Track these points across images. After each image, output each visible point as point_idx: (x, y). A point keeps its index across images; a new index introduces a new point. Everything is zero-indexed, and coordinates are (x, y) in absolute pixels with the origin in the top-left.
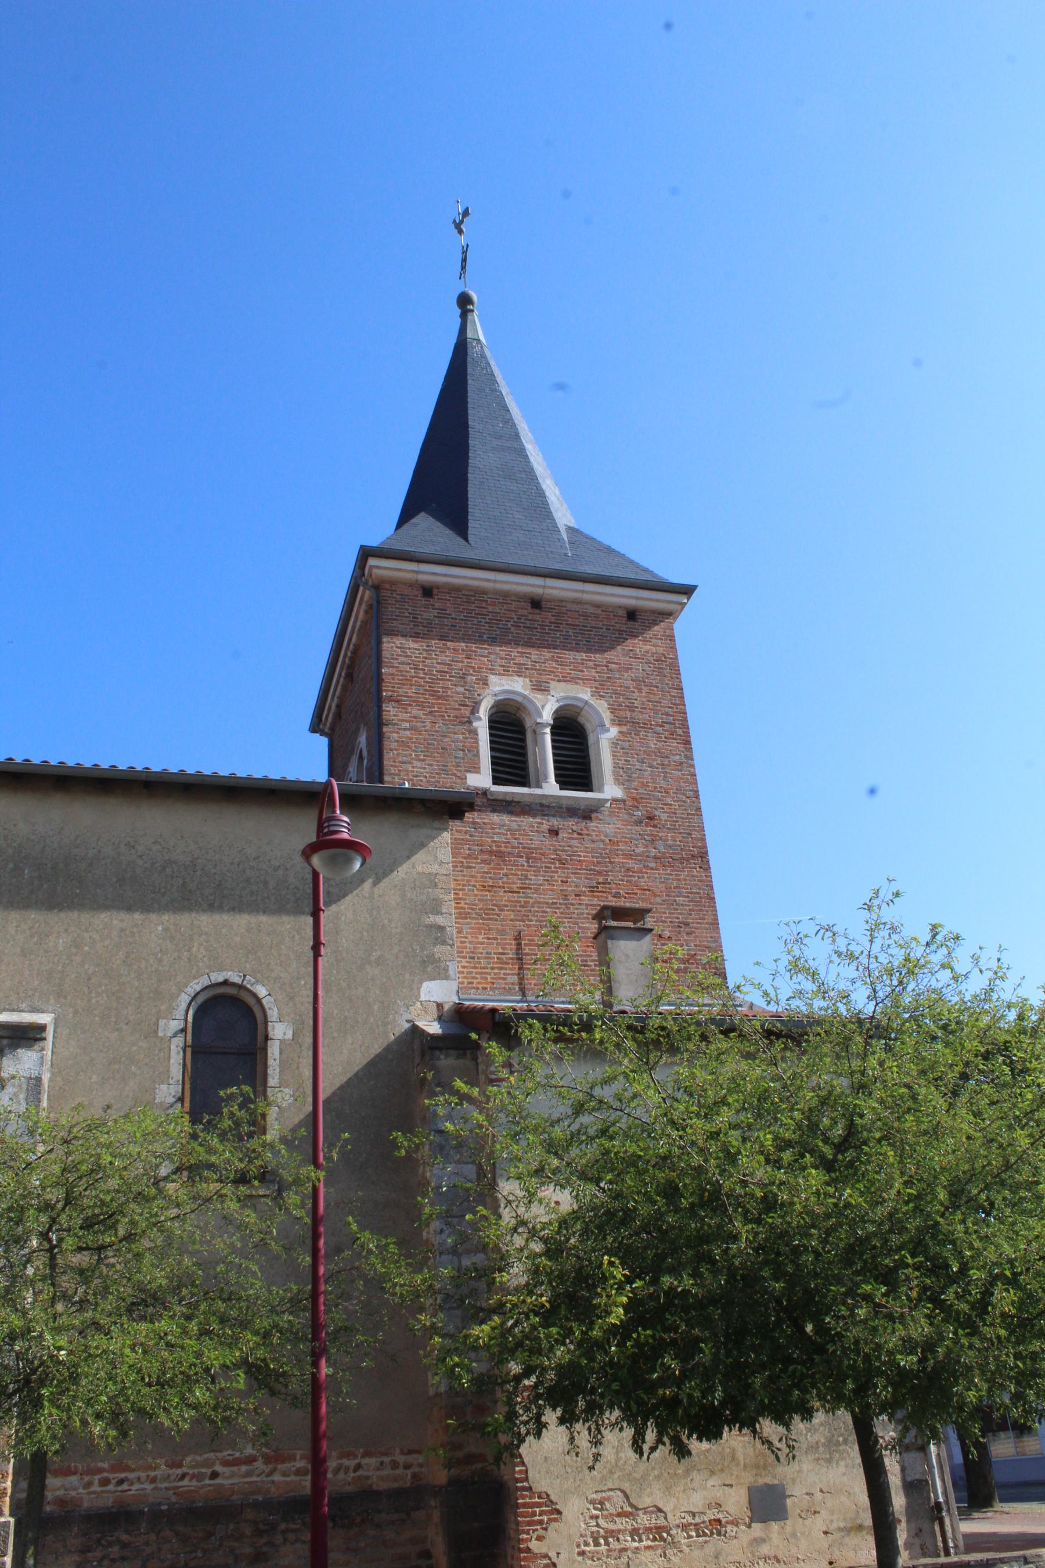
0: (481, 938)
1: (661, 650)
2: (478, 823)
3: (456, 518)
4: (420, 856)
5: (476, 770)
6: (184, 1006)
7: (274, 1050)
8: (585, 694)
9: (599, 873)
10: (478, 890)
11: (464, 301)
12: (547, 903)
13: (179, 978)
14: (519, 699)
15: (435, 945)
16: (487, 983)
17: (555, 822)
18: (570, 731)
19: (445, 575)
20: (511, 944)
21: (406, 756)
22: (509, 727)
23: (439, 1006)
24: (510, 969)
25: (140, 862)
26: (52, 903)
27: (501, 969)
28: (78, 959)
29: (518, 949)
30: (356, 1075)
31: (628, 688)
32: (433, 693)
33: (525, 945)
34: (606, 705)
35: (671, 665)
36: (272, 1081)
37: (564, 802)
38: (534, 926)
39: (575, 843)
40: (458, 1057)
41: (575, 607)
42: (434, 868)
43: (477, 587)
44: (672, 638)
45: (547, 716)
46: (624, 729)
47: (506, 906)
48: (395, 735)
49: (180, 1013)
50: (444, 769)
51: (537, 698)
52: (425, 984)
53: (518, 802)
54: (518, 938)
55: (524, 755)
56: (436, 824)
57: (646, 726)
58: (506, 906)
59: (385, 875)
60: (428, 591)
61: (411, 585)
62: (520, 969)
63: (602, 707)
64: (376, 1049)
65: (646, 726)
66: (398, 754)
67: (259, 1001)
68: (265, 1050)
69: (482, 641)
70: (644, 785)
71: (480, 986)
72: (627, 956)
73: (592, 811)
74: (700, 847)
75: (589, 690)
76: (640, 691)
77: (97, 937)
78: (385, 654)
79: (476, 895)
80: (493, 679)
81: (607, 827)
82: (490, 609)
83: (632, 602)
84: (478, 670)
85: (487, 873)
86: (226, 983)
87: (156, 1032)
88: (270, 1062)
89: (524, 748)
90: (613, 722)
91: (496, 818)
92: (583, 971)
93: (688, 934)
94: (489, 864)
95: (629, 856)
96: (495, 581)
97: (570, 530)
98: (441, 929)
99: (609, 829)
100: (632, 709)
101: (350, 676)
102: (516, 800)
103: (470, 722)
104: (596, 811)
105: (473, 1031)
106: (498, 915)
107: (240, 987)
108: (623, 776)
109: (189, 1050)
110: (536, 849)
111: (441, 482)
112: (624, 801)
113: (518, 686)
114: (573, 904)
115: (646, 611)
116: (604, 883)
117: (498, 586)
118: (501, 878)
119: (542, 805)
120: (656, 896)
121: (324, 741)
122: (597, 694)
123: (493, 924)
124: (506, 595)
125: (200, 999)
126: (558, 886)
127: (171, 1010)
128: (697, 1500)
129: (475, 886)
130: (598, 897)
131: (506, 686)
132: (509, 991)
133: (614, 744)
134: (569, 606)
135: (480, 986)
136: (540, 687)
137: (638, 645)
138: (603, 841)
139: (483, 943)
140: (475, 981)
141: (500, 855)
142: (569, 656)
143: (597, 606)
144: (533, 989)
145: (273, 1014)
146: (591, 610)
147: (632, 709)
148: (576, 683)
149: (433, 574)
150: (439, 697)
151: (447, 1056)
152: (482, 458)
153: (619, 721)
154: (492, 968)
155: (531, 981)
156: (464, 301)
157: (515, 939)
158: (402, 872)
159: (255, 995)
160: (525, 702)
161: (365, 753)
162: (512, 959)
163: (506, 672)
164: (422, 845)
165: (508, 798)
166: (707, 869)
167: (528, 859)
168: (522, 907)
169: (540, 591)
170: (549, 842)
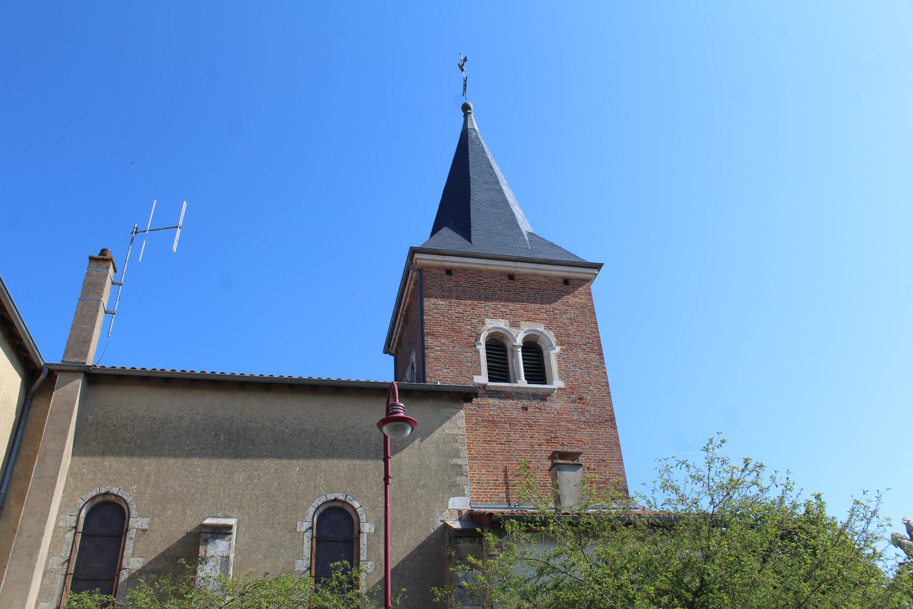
0: (483, 471)
3: (465, 231)
4: (447, 424)
5: (479, 373)
6: (311, 513)
7: (364, 539)
8: (541, 328)
9: (552, 432)
11: (466, 108)
13: (309, 497)
14: (503, 332)
15: (456, 476)
17: (525, 402)
18: (533, 349)
22: (497, 348)
23: (460, 512)
25: (287, 430)
26: (237, 455)
28: (251, 487)
30: (412, 553)
32: (453, 330)
36: (362, 558)
37: (530, 391)
39: (537, 414)
40: (471, 542)
41: (533, 278)
42: (456, 431)
44: (590, 294)
45: (519, 341)
46: (564, 347)
49: (309, 518)
51: (513, 331)
52: (451, 499)
54: (505, 471)
55: (507, 364)
56: (456, 405)
57: (577, 345)
59: (427, 436)
60: (449, 272)
61: (439, 268)
63: (551, 335)
64: (423, 537)
65: (577, 345)
67: (355, 510)
68: (358, 539)
69: (480, 299)
70: (577, 380)
72: (569, 480)
76: (573, 325)
77: (261, 474)
78: (426, 308)
80: (487, 321)
81: (556, 405)
82: (485, 280)
83: (566, 274)
84: (479, 316)
86: (335, 500)
87: (295, 529)
88: (362, 546)
89: (506, 360)
90: (557, 344)
91: (491, 401)
95: (570, 422)
97: (529, 233)
98: (460, 466)
99: (557, 406)
100: (568, 335)
101: (406, 321)
103: (475, 346)
104: (549, 395)
105: (479, 525)
107: (344, 502)
108: (564, 374)
109: (314, 540)
111: (455, 209)
113: (502, 324)
117: (490, 268)
119: (518, 393)
121: (392, 358)
122: (548, 328)
123: (491, 463)
124: (493, 273)
125: (321, 510)
126: (528, 440)
127: (304, 516)
131: (493, 324)
132: (500, 502)
133: (558, 356)
136: (515, 325)
137: (570, 299)
141: (494, 422)
142: (532, 306)
145: (363, 518)
146: (543, 279)
147: (568, 335)
150: (456, 332)
151: (464, 542)
152: (478, 195)
153: (560, 343)
156: (466, 108)
158: (437, 434)
159: (353, 507)
160: (506, 334)
161: (415, 365)
163: (495, 316)
164: (449, 418)
166: (615, 428)
167: (510, 424)
169: (513, 269)
170: (522, 414)
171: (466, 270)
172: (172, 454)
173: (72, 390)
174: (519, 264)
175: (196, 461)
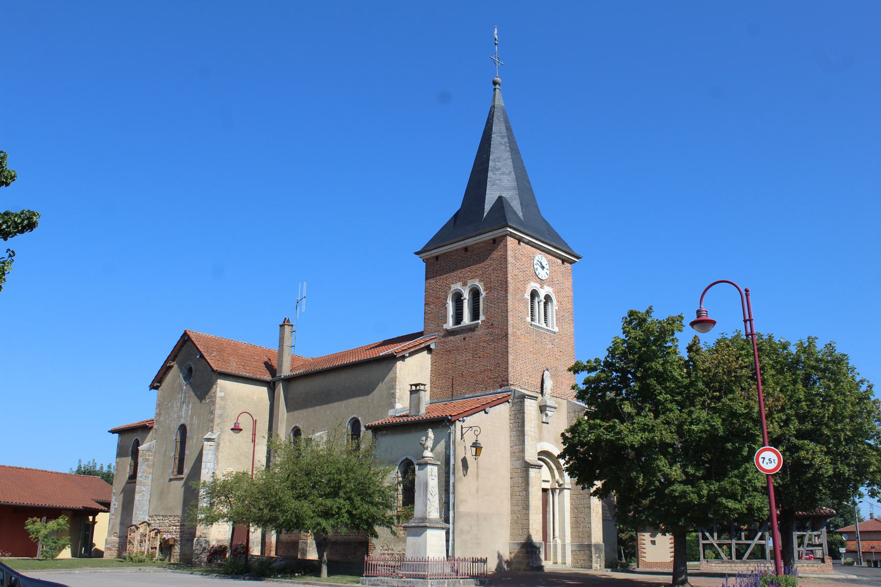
17: (465, 335)
26: (327, 402)
60: (437, 258)
61: (433, 258)
90: (485, 290)
113: (458, 286)
124: (457, 250)
128: (400, 548)
136: (465, 284)
137: (496, 254)
141: (450, 351)
142: (474, 267)
143: (484, 242)
171: (445, 254)
172: (311, 407)
173: (280, 388)
175: (317, 408)
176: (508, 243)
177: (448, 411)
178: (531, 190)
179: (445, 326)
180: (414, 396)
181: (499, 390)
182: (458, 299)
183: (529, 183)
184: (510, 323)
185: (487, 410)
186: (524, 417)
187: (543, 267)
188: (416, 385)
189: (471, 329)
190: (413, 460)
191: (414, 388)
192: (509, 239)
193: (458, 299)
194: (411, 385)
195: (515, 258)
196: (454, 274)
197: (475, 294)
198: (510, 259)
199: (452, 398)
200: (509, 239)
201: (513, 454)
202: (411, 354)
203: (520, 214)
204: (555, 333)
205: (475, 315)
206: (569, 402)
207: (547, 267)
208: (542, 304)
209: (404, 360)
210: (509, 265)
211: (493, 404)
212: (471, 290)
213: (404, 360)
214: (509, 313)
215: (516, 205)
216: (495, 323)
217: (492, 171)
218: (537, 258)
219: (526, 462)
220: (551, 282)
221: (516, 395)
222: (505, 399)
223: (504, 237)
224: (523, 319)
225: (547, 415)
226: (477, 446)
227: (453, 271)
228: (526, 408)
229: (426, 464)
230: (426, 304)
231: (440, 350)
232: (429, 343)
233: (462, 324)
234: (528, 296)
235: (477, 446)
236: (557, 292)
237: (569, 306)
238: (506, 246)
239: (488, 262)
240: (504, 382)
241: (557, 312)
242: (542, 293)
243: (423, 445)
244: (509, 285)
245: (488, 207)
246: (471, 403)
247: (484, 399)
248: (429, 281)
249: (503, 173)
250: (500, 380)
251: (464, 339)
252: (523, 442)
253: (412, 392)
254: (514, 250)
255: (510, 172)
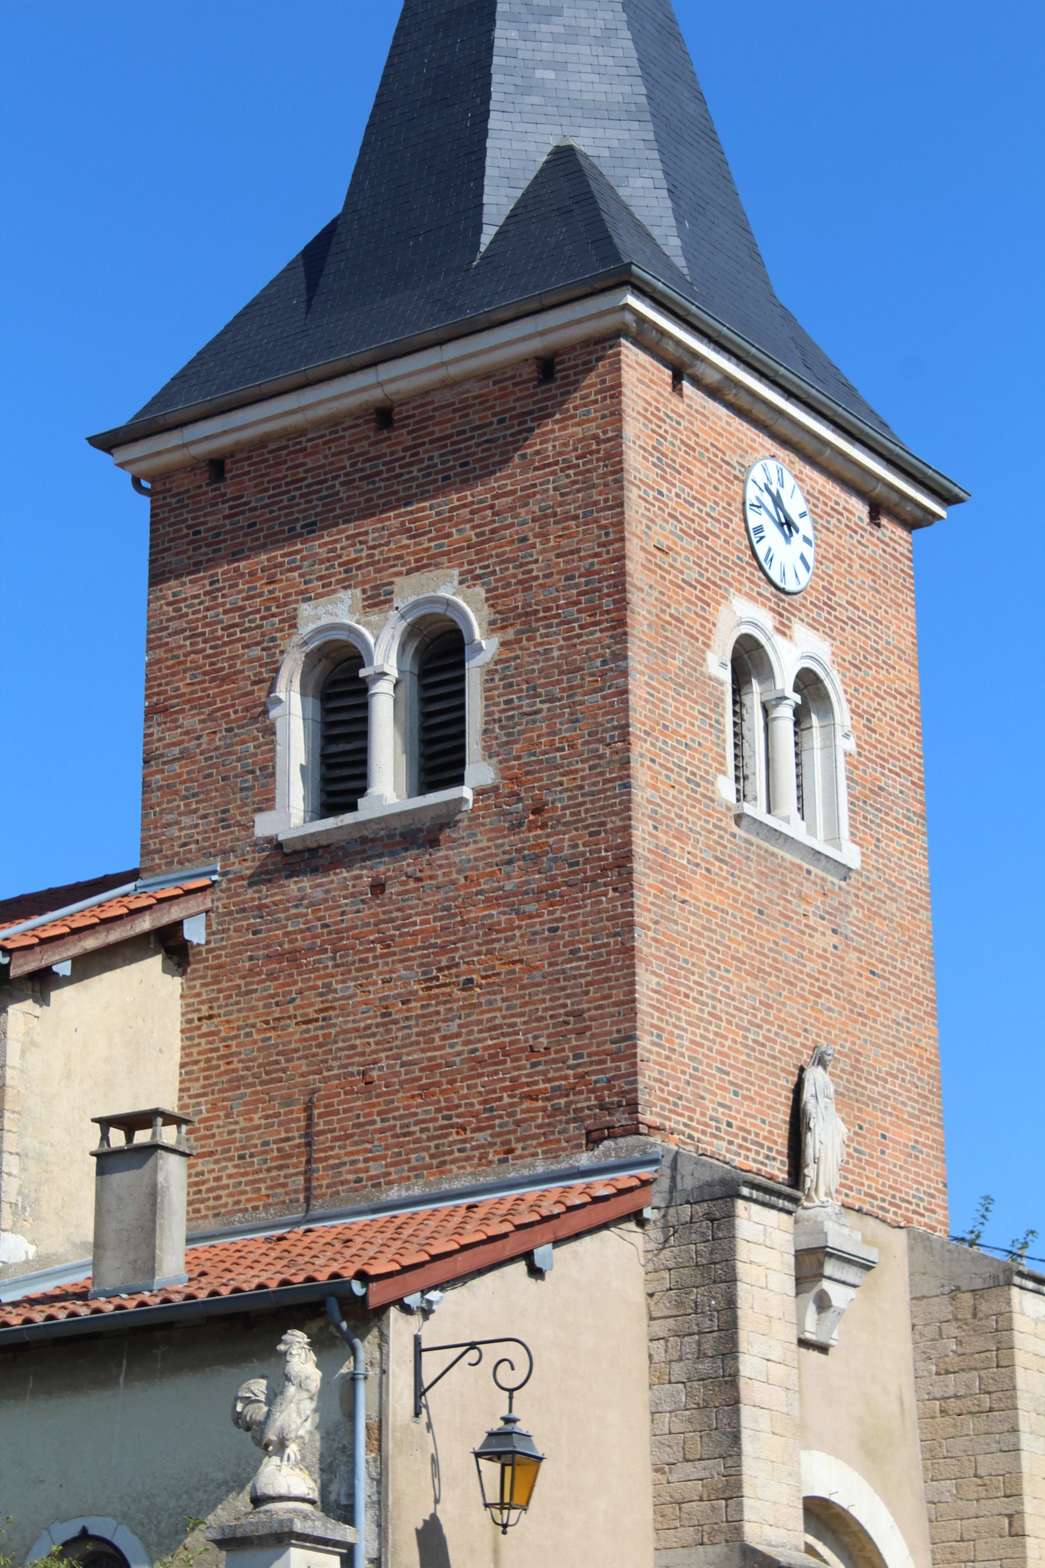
1: (592, 428)
2: (266, 906)
9: (443, 949)
10: (259, 1031)
12: (357, 1030)
16: (259, 1199)
17: (383, 868)
19: (225, 433)
20: (298, 1120)
21: (171, 811)
24: (295, 1166)
27: (280, 1168)
29: (308, 1126)
31: (525, 539)
33: (320, 1116)
34: (483, 595)
35: (608, 456)
37: (395, 824)
38: (337, 1077)
41: (449, 396)
43: (285, 429)
46: (510, 634)
47: (296, 1050)
48: (158, 777)
50: (225, 822)
53: (329, 846)
54: (308, 1108)
58: (296, 1050)
60: (216, 467)
61: (192, 467)
62: (308, 1162)
66: (162, 811)
69: (291, 539)
71: (249, 1206)
72: (120, 1198)
73: (441, 828)
74: (618, 847)
75: (456, 572)
76: (544, 536)
79: (255, 1042)
80: (306, 610)
83: (536, 345)
85: (272, 996)
90: (493, 627)
92: (400, 1145)
93: (580, 1033)
94: (277, 979)
95: (491, 902)
96: (302, 409)
102: (324, 843)
103: (265, 712)
104: (448, 825)
106: (284, 1070)
110: (348, 929)
112: (495, 789)
113: (339, 611)
114: (395, 1022)
115: (573, 348)
116: (448, 968)
117: (312, 414)
118: (293, 1000)
119: (364, 840)
120: (531, 969)
123: (279, 1091)
124: (334, 422)
129: (253, 1026)
130: (437, 996)
133: (490, 674)
134: (439, 399)
135: (249, 1206)
136: (377, 599)
137: (554, 437)
138: (453, 882)
139: (258, 1127)
140: (243, 1198)
141: (293, 957)
142: (427, 510)
144: (324, 1195)
146: (475, 389)
147: (525, 585)
148: (437, 565)
149: (206, 438)
150: (224, 680)
154: (269, 1170)
155: (323, 1178)
157: (305, 1110)
162: (298, 1146)
165: (312, 844)
167: (335, 951)
168: (320, 1046)
169: (377, 394)
171: (261, 444)
174: (387, 371)
176: (629, 376)
177: (320, 1254)
178: (712, 138)
179: (265, 826)
180: (119, 1179)
181: (584, 1159)
182: (339, 685)
183: (699, 97)
184: (641, 795)
185: (542, 1254)
186: (731, 1304)
187: (787, 525)
188: (130, 1123)
189: (418, 835)
190: (126, 1542)
191: (117, 1138)
192: (630, 354)
193: (339, 685)
194: (105, 1123)
195: (659, 457)
196: (317, 546)
197: (438, 651)
198: (636, 462)
199: (308, 1205)
200: (630, 354)
201: (668, 1508)
202: (89, 965)
203: (672, 245)
204: (845, 872)
205: (438, 758)
206: (919, 1242)
207: (805, 526)
208: (785, 714)
209: (43, 999)
210: (633, 495)
211: (572, 1226)
212: (412, 632)
213: (43, 999)
214: (639, 749)
215: (642, 193)
216: (558, 800)
217: (513, 19)
218: (757, 474)
219: (749, 1553)
220: (819, 606)
221: (687, 1183)
222: (626, 1204)
223: (602, 345)
224: (698, 784)
225: (823, 1303)
226: (509, 1453)
227: (311, 528)
228: (743, 1251)
229: (283, 1538)
230: (151, 712)
231: (237, 949)
232: (174, 913)
233: (367, 809)
234: (719, 667)
235: (509, 1453)
236: (851, 666)
237: (907, 741)
238: (615, 391)
239: (510, 478)
240: (612, 1113)
241: (852, 766)
242: (786, 659)
243: (255, 1430)
244: (634, 597)
245: (498, 200)
246: (439, 1228)
247: (496, 1210)
248: (171, 588)
249: (573, 34)
250: (585, 1101)
251: (378, 887)
252: (729, 1442)
253: (107, 1161)
254: (653, 416)
255: (609, 31)
